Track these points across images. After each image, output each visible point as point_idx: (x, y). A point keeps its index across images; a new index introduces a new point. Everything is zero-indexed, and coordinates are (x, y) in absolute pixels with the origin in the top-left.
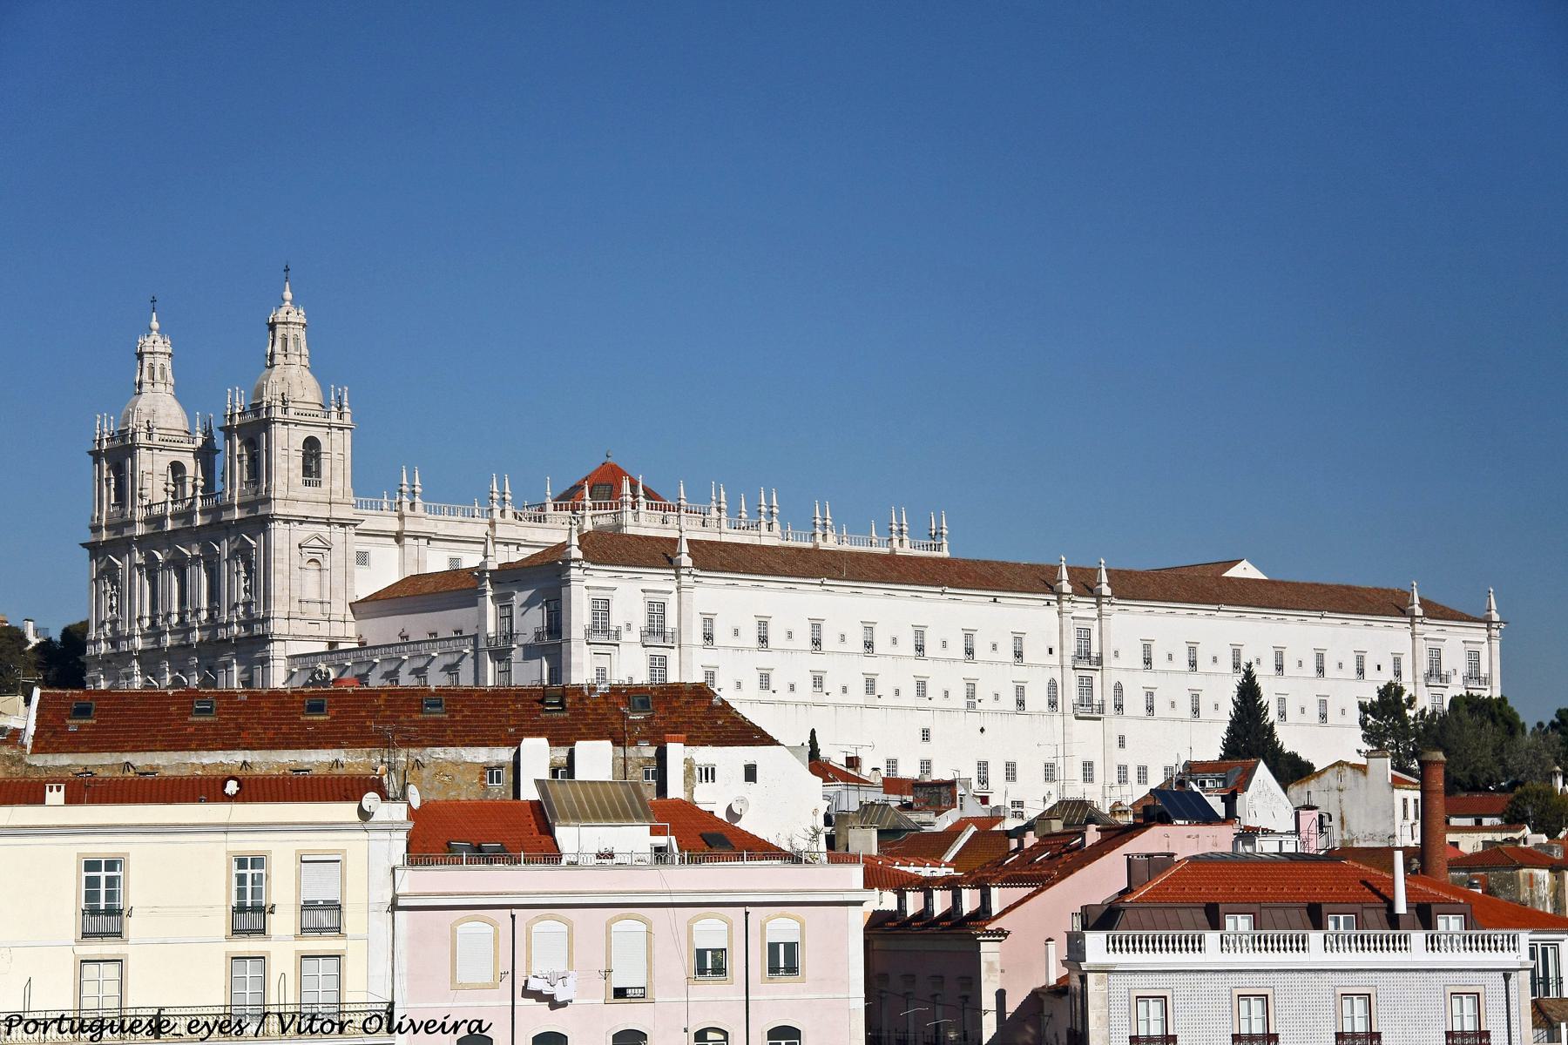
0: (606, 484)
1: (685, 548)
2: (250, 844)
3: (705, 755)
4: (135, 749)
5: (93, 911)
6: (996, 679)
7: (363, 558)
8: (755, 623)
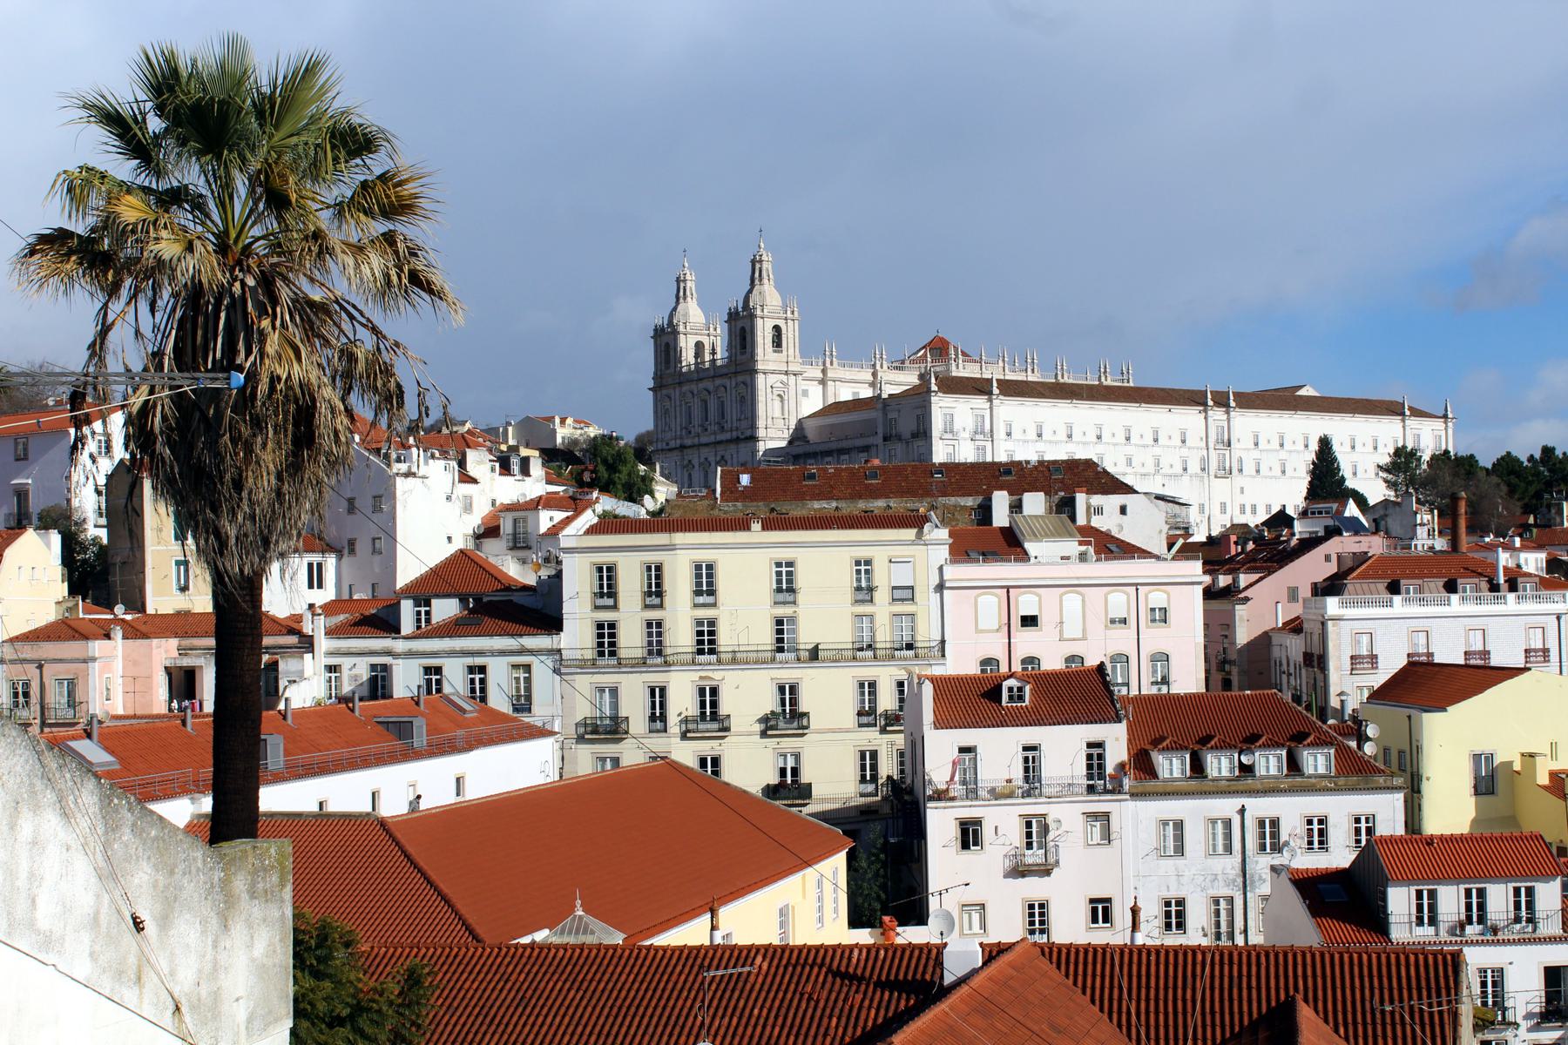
0: (939, 348)
1: (995, 384)
2: (863, 553)
3: (1097, 500)
4: (776, 500)
5: (779, 590)
6: (1172, 458)
7: (805, 393)
8: (1034, 426)
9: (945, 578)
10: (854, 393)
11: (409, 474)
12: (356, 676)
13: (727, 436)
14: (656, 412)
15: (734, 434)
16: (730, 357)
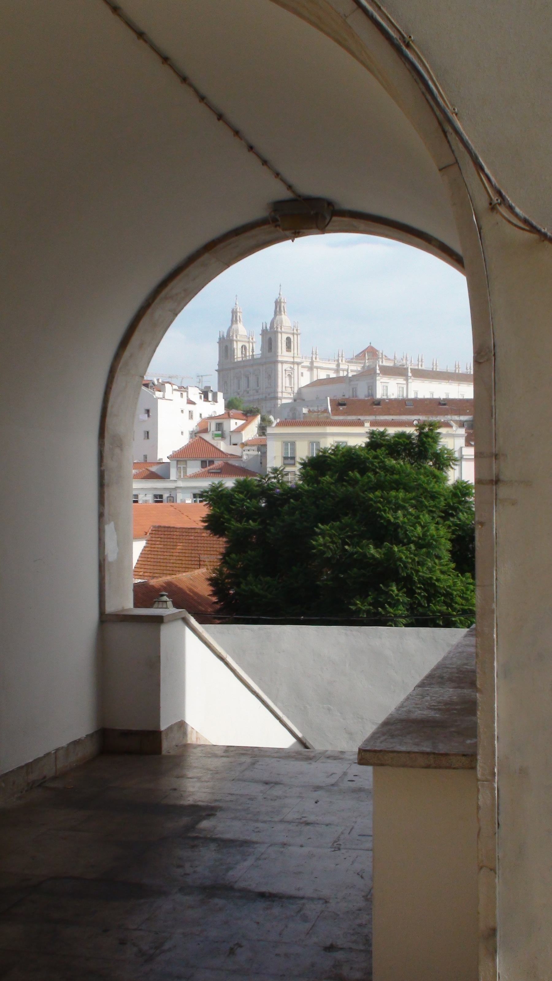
1: (409, 370)
9: (463, 454)
10: (327, 375)
11: (163, 398)
12: (146, 501)
16: (262, 354)
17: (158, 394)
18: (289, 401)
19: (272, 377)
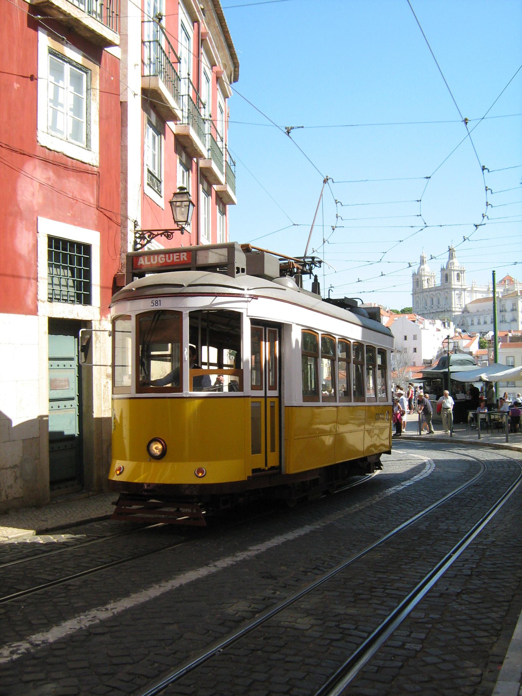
11: (424, 328)
13: (441, 310)
14: (413, 302)
15: (443, 310)
17: (421, 326)
18: (460, 313)
19: (448, 299)
